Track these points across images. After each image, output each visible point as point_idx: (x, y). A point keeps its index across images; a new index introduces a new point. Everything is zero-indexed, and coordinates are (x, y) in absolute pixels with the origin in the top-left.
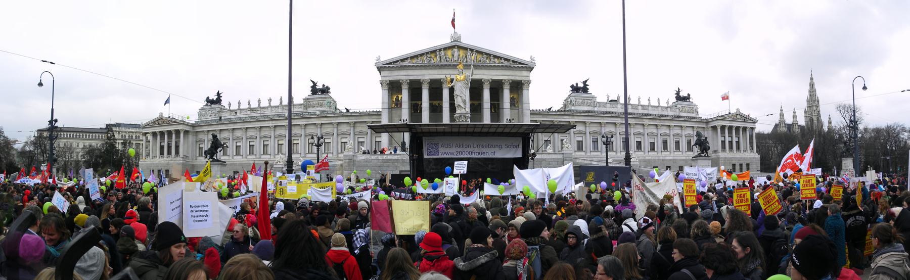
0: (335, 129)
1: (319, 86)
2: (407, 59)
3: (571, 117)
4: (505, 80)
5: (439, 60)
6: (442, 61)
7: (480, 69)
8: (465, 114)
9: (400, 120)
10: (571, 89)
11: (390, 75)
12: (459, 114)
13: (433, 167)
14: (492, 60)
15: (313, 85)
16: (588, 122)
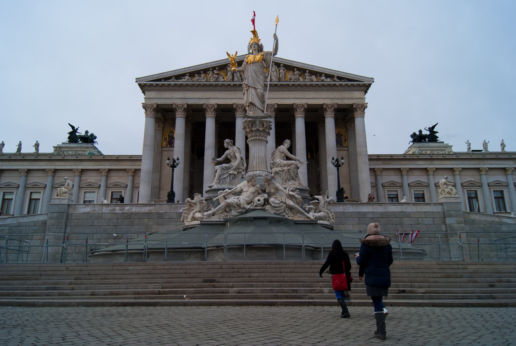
0: (77, 179)
1: (81, 132)
2: (184, 75)
3: (428, 162)
4: (327, 105)
5: (231, 77)
6: (236, 79)
7: (290, 91)
8: (262, 117)
9: (169, 159)
10: (412, 140)
11: (158, 96)
12: (250, 117)
13: (198, 215)
14: (307, 77)
15: (71, 130)
16: (458, 168)
